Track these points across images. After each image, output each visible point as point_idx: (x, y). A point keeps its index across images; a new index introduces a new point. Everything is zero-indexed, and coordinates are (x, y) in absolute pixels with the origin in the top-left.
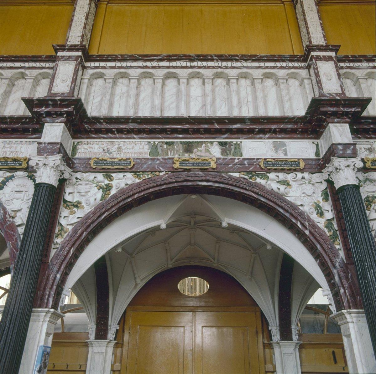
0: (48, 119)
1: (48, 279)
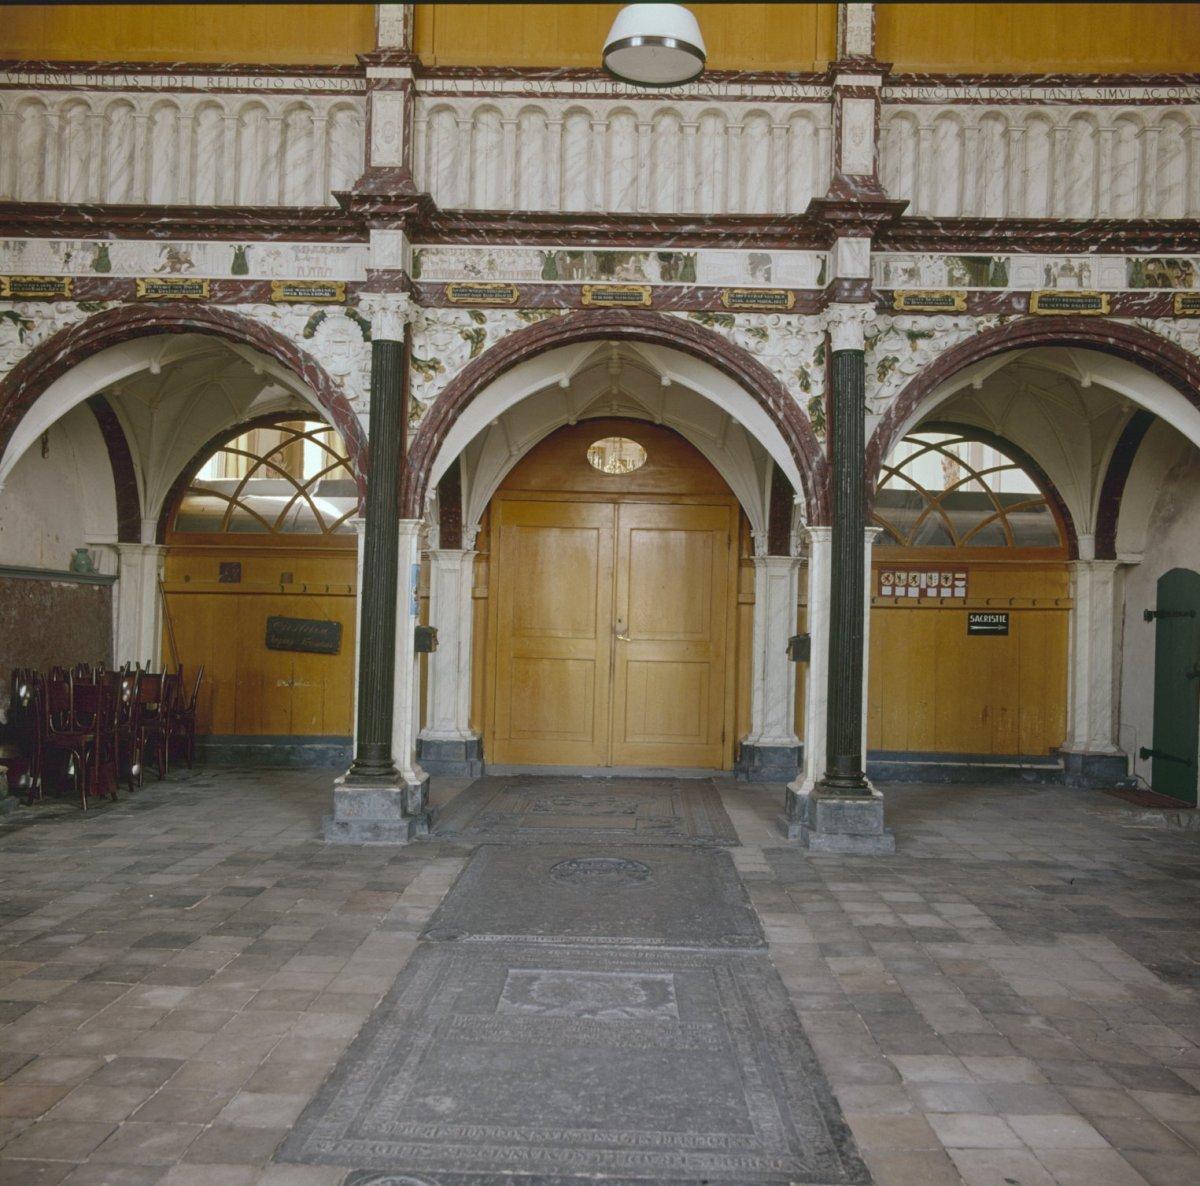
0: (374, 223)
1: (409, 479)
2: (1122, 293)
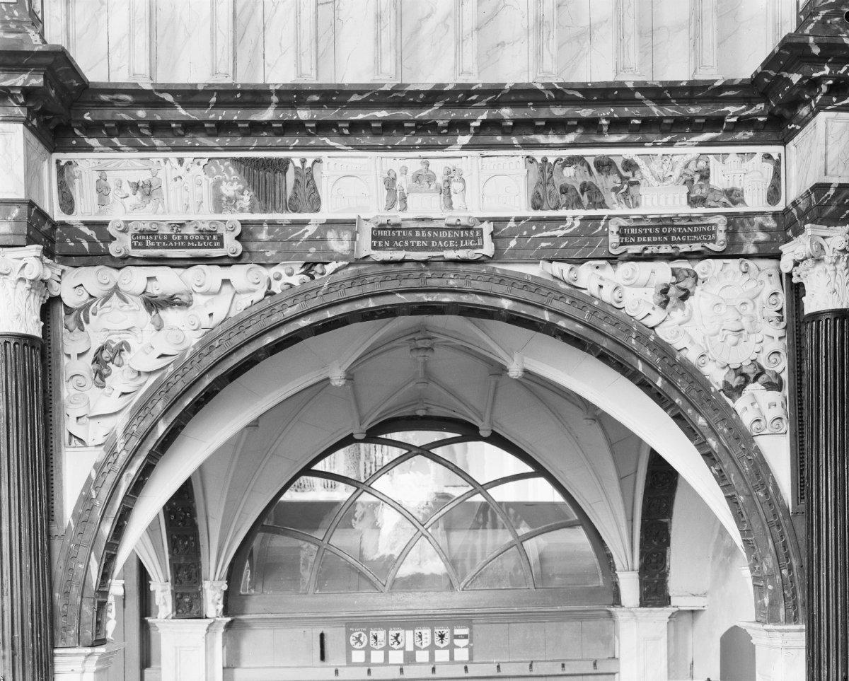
2: (518, 220)
